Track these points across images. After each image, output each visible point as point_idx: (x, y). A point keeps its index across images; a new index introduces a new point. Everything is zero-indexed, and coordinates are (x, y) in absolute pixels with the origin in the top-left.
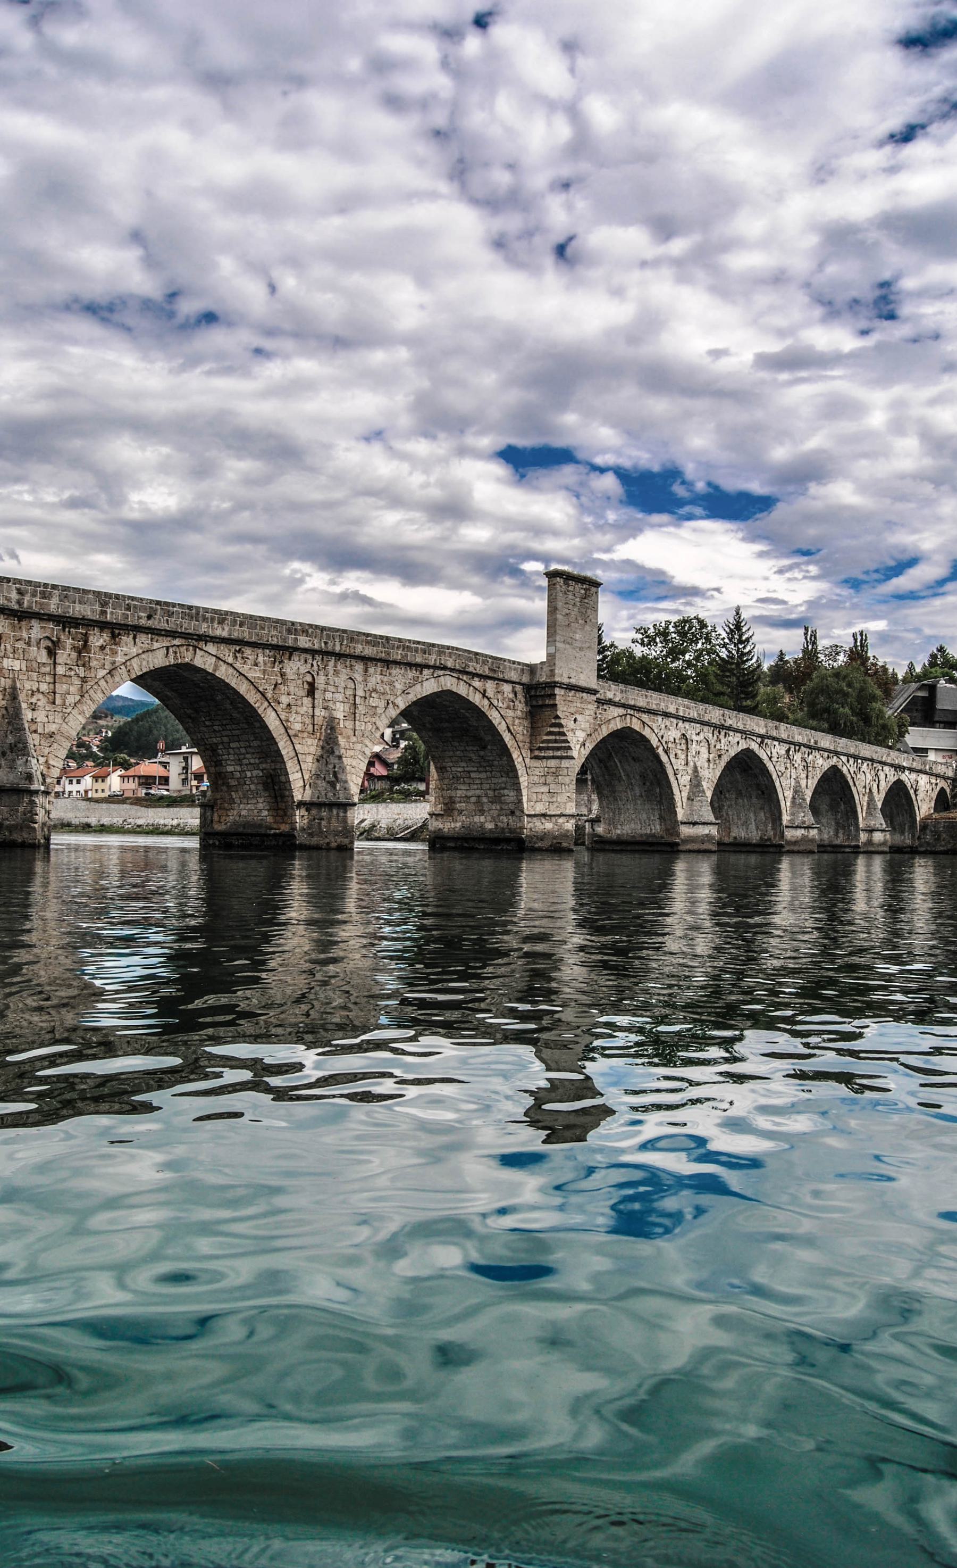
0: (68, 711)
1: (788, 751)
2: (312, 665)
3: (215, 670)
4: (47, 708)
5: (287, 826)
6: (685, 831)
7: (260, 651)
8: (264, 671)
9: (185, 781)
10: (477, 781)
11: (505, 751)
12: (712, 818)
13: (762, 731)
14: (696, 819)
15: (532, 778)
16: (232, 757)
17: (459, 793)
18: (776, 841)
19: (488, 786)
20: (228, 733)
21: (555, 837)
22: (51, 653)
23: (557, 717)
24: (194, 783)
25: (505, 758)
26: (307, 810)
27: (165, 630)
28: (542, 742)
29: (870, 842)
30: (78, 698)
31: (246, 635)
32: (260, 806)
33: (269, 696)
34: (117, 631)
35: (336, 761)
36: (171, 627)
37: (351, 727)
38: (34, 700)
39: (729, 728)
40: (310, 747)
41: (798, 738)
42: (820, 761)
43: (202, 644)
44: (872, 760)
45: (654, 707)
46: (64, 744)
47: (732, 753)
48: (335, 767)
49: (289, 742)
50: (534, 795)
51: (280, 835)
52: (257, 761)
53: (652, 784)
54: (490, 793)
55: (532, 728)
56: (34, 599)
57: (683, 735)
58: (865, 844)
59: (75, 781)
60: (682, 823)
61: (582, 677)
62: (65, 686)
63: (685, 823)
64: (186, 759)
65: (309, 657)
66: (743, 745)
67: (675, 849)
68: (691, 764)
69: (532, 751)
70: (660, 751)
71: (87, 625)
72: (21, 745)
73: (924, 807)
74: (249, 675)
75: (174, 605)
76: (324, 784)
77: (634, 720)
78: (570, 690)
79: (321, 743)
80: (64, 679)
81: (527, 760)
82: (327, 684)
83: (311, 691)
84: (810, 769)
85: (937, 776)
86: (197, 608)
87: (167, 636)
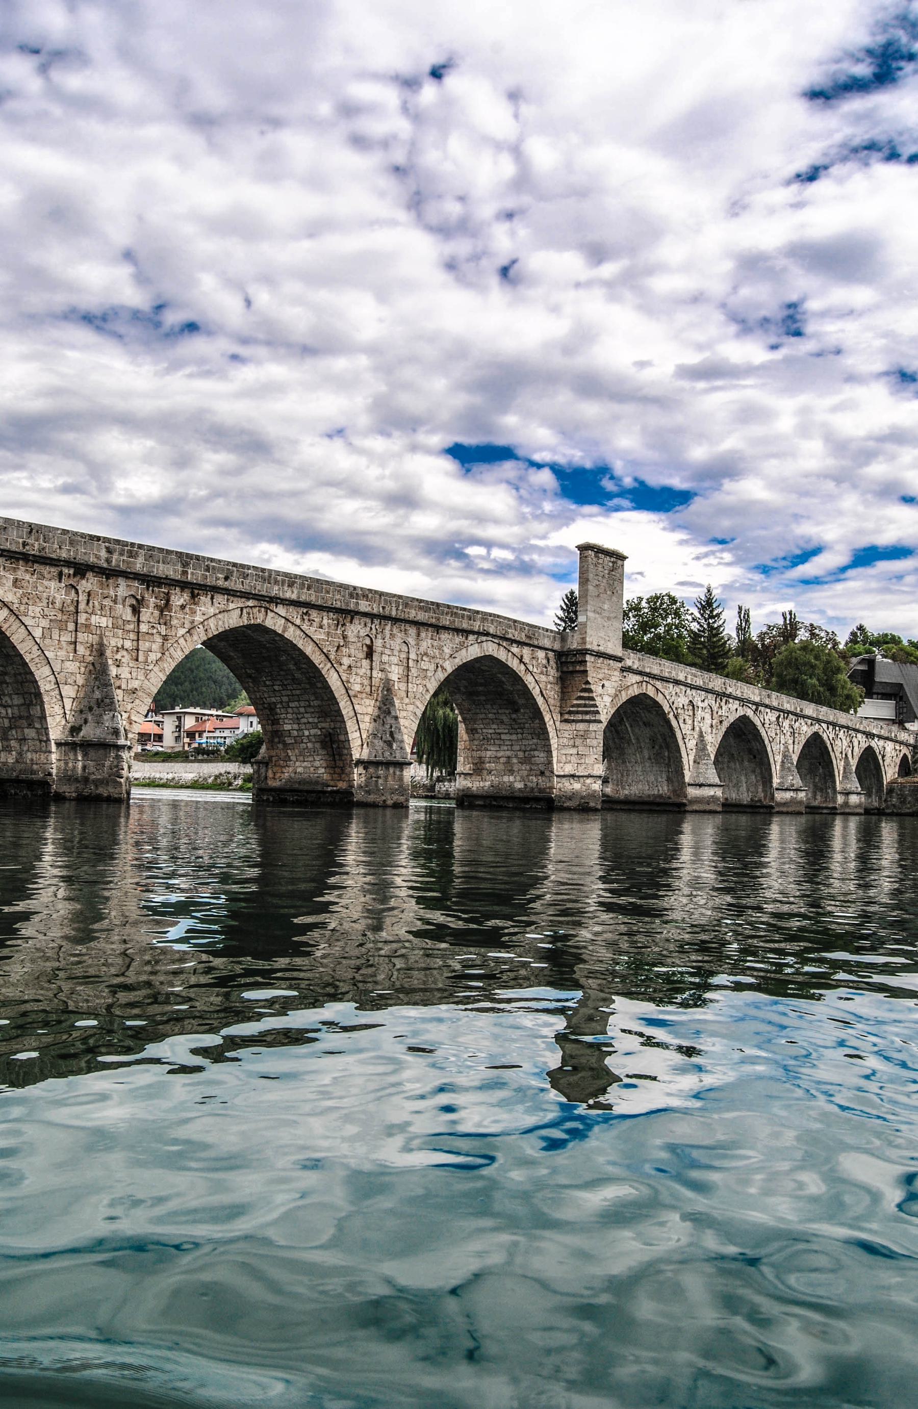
0: (150, 668)
1: (779, 717)
2: (371, 629)
3: (284, 631)
4: (131, 665)
5: (345, 783)
6: (692, 792)
7: (325, 614)
8: (328, 634)
9: (177, 739)
10: (508, 743)
11: (537, 714)
12: (717, 780)
13: (757, 699)
14: (702, 780)
15: (561, 740)
16: (289, 716)
17: (489, 754)
18: (766, 802)
19: (518, 748)
20: (289, 693)
21: (582, 797)
22: (136, 611)
23: (588, 683)
24: (187, 740)
25: (537, 721)
26: (365, 768)
27: (241, 592)
28: (573, 706)
29: (846, 804)
30: (159, 655)
31: (313, 598)
32: (317, 764)
33: (332, 657)
34: (196, 591)
35: (393, 721)
36: (246, 588)
37: (404, 688)
38: (118, 657)
39: (729, 696)
40: (367, 707)
41: (787, 706)
42: (805, 728)
43: (273, 607)
44: (848, 728)
45: (667, 675)
46: (145, 700)
47: (732, 719)
48: (391, 727)
49: (349, 703)
50: (564, 757)
51: (337, 792)
52: (316, 721)
53: (661, 747)
54: (521, 754)
55: (563, 692)
56: (122, 558)
57: (691, 701)
58: (842, 806)
60: (689, 785)
61: (610, 645)
62: (147, 644)
63: (692, 785)
64: (179, 718)
65: (368, 621)
66: (741, 712)
67: (683, 809)
68: (697, 729)
69: (561, 714)
70: (671, 716)
71: (170, 585)
72: (108, 701)
73: (890, 773)
74: (315, 637)
75: (249, 567)
76: (381, 743)
77: (650, 687)
78: (600, 657)
79: (378, 704)
80: (147, 637)
81: (558, 723)
82: (384, 647)
83: (370, 654)
84: (796, 735)
85: (901, 743)
86: (270, 571)
87: (241, 597)
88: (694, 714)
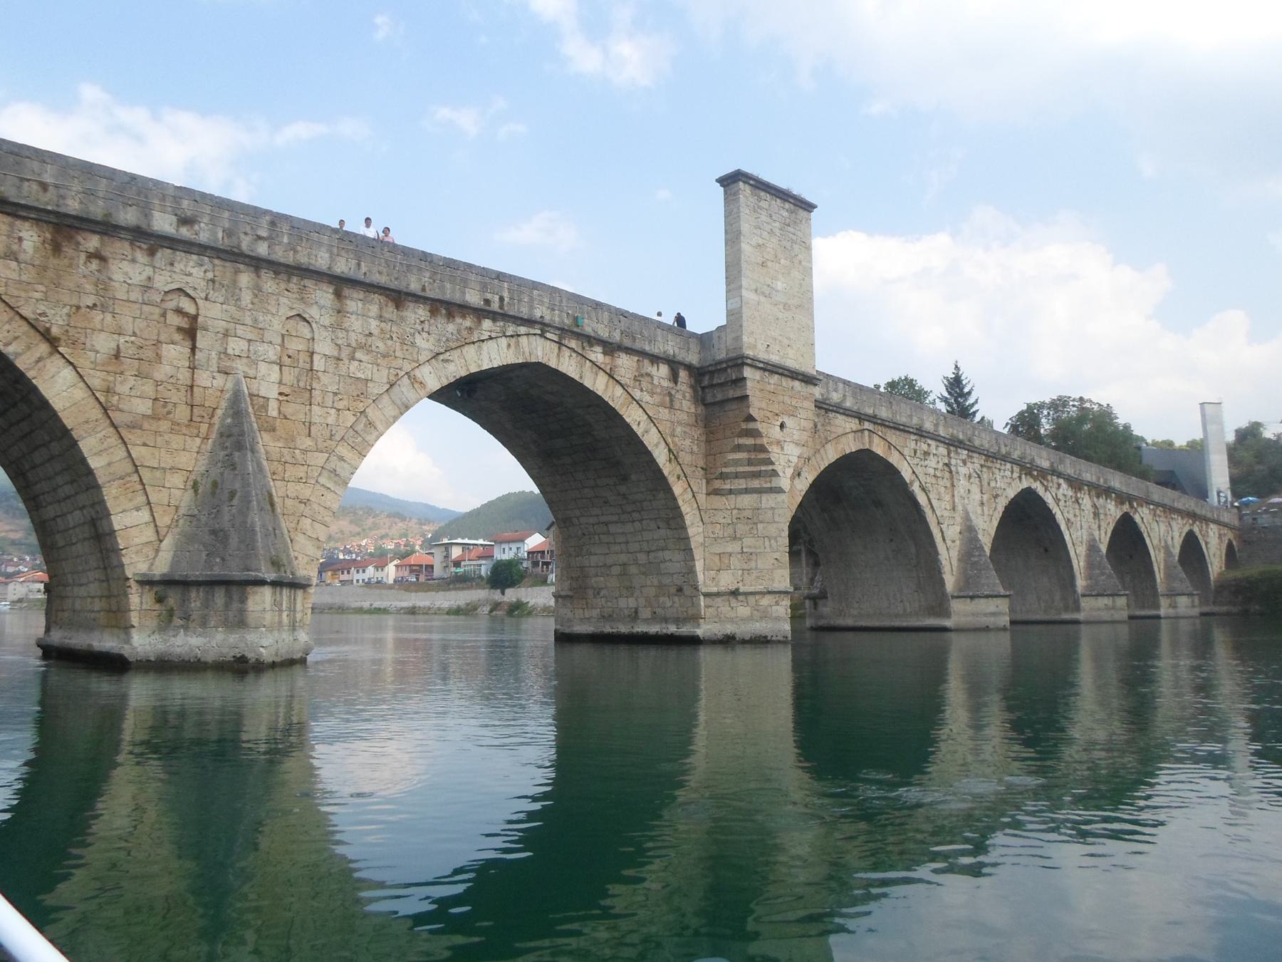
10: (622, 539)
11: (659, 481)
13: (1045, 464)
17: (594, 560)
23: (750, 418)
25: (661, 495)
41: (1087, 476)
49: (114, 440)
50: (716, 559)
54: (642, 558)
55: (708, 441)
59: (361, 571)
60: (953, 597)
61: (791, 353)
64: (447, 550)
68: (960, 508)
70: (916, 488)
73: (1215, 564)
77: (876, 439)
84: (1102, 517)
85: (1225, 525)
88: (953, 485)
